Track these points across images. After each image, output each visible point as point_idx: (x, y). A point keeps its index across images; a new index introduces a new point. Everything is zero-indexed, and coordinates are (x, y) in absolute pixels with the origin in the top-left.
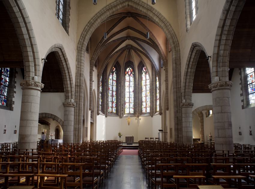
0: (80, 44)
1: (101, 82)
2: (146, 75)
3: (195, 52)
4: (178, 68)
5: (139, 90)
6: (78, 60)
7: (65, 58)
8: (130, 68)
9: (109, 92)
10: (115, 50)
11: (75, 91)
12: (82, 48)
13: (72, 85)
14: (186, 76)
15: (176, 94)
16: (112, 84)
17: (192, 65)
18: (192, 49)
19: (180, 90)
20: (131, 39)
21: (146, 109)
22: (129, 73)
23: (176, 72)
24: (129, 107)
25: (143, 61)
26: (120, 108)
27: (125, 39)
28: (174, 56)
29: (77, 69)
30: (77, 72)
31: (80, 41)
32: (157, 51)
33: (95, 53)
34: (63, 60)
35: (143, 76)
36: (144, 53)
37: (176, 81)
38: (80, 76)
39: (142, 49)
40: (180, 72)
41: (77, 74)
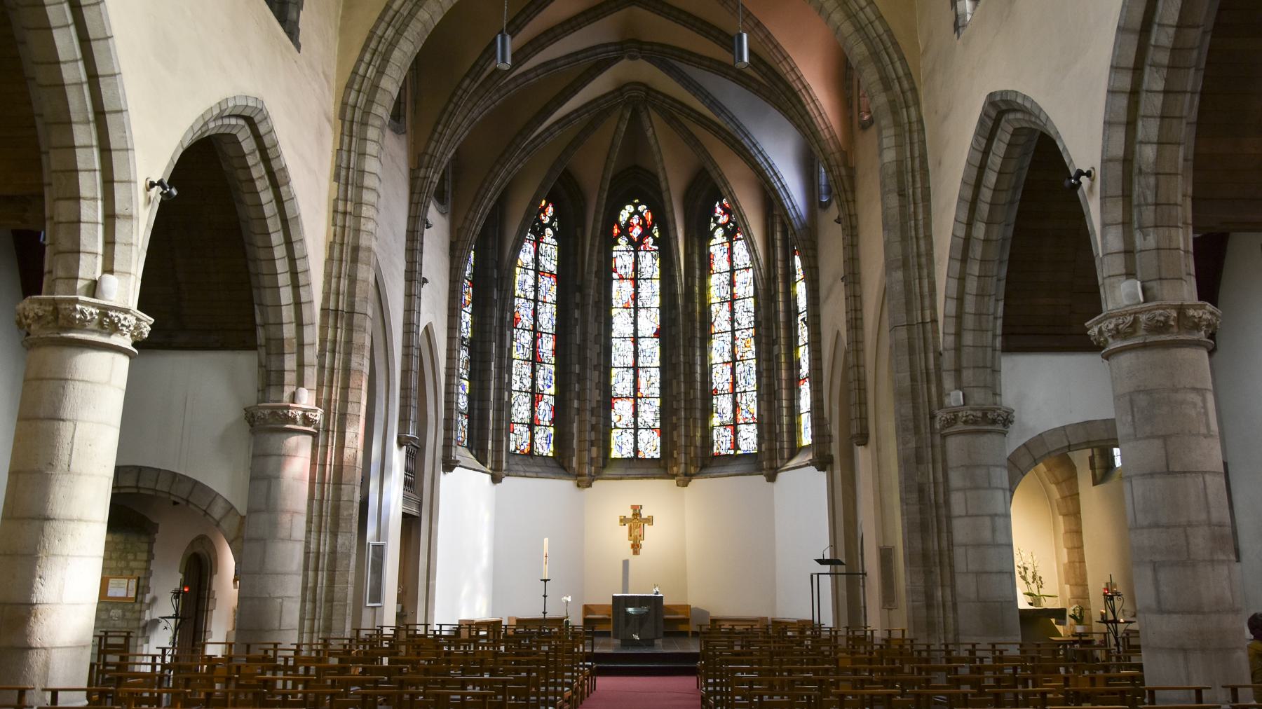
0: (356, 87)
3: (1004, 136)
4: (916, 220)
5: (694, 328)
6: (343, 173)
7: (275, 166)
8: (636, 206)
9: (512, 339)
11: (323, 341)
12: (367, 113)
13: (305, 309)
14: (964, 260)
15: (907, 357)
17: (993, 204)
18: (990, 124)
19: (930, 335)
20: (643, 58)
21: (735, 433)
22: (636, 232)
23: (904, 239)
24: (636, 423)
25: (716, 167)
26: (580, 431)
27: (613, 54)
28: (890, 156)
29: (335, 225)
30: (338, 240)
31: (361, 71)
32: (791, 119)
33: (440, 128)
34: (262, 177)
35: (712, 250)
36: (719, 126)
37: (907, 284)
38: (355, 260)
39: (709, 107)
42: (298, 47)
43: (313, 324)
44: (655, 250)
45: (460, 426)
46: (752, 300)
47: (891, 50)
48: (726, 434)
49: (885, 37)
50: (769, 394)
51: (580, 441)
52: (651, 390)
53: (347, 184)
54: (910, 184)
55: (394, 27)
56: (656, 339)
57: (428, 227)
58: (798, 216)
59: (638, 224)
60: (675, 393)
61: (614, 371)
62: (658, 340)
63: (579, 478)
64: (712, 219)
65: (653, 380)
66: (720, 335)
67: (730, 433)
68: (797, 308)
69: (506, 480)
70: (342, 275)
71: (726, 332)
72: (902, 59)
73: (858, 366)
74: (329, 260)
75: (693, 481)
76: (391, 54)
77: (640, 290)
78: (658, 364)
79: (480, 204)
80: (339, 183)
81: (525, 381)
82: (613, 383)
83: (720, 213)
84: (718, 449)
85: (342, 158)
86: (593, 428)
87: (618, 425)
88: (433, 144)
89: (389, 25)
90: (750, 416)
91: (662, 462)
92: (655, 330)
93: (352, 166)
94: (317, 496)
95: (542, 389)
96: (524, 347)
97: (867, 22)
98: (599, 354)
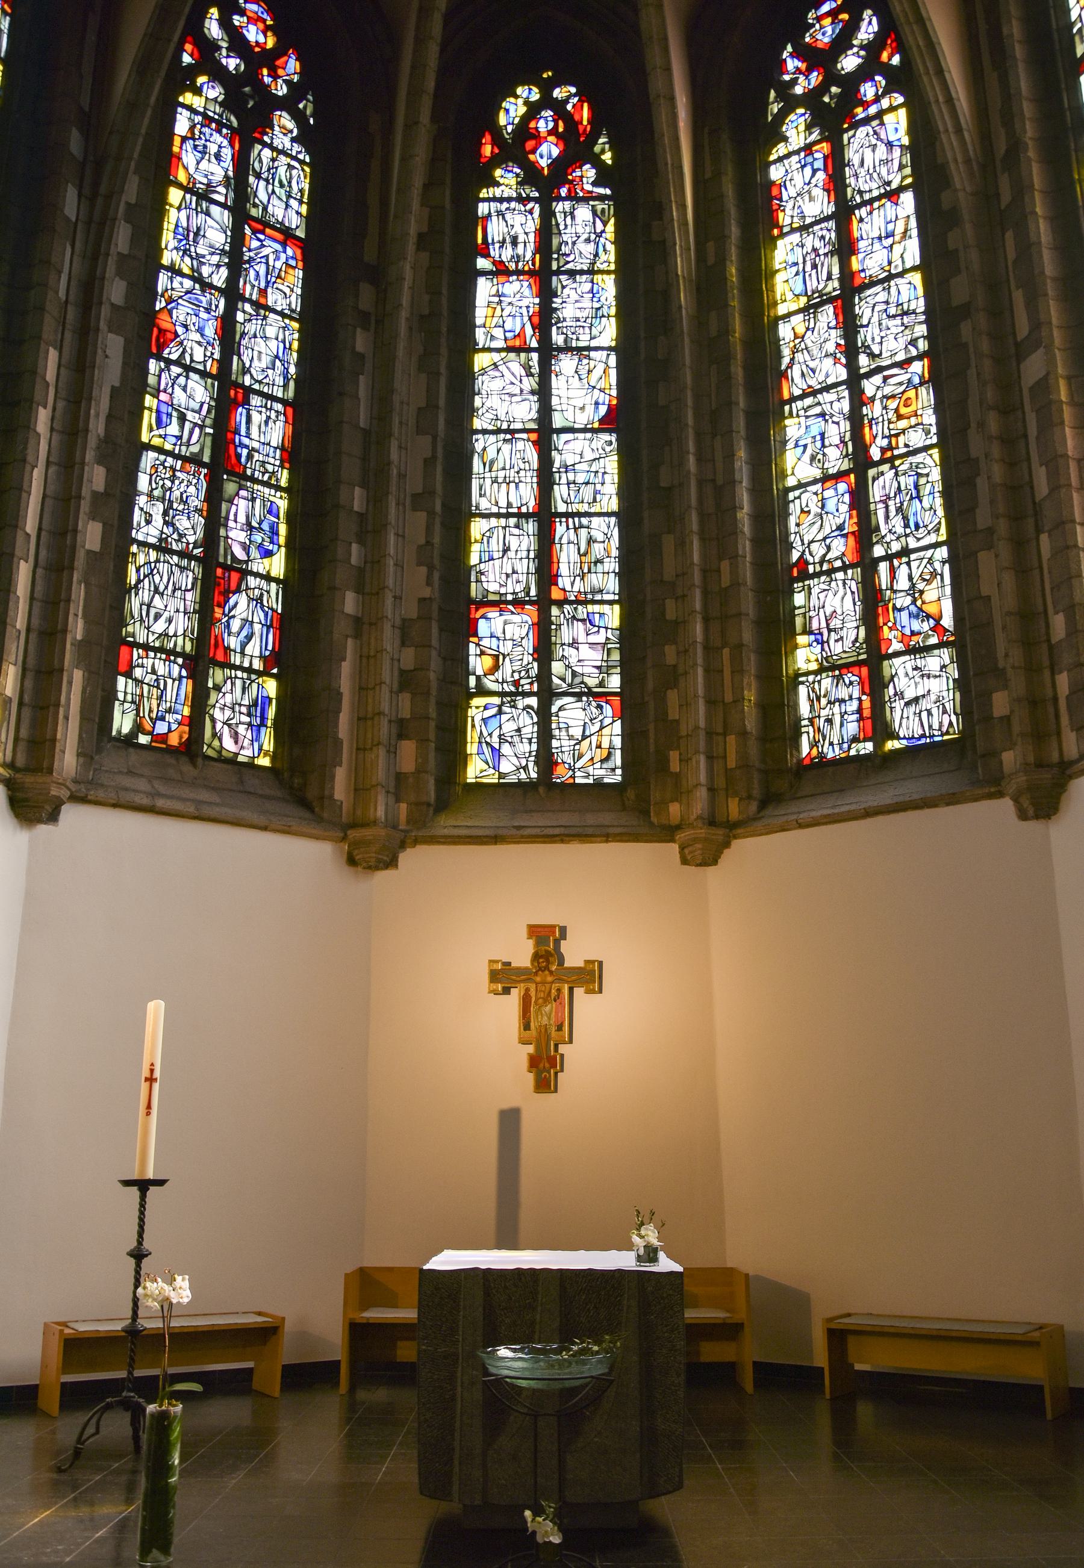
5: (726, 378)
8: (546, 88)
22: (547, 153)
24: (544, 676)
44: (601, 198)
46: (917, 278)
48: (843, 693)
50: (1016, 518)
52: (595, 580)
56: (606, 437)
59: (553, 132)
60: (669, 574)
61: (477, 528)
62: (613, 438)
63: (353, 834)
64: (773, 94)
65: (598, 550)
66: (809, 401)
67: (856, 692)
71: (827, 389)
75: (736, 844)
78: (613, 504)
81: (183, 523)
82: (474, 559)
83: (798, 70)
84: (814, 744)
86: (407, 681)
91: (631, 794)
92: (603, 410)
95: (240, 554)
96: (182, 419)
98: (429, 463)
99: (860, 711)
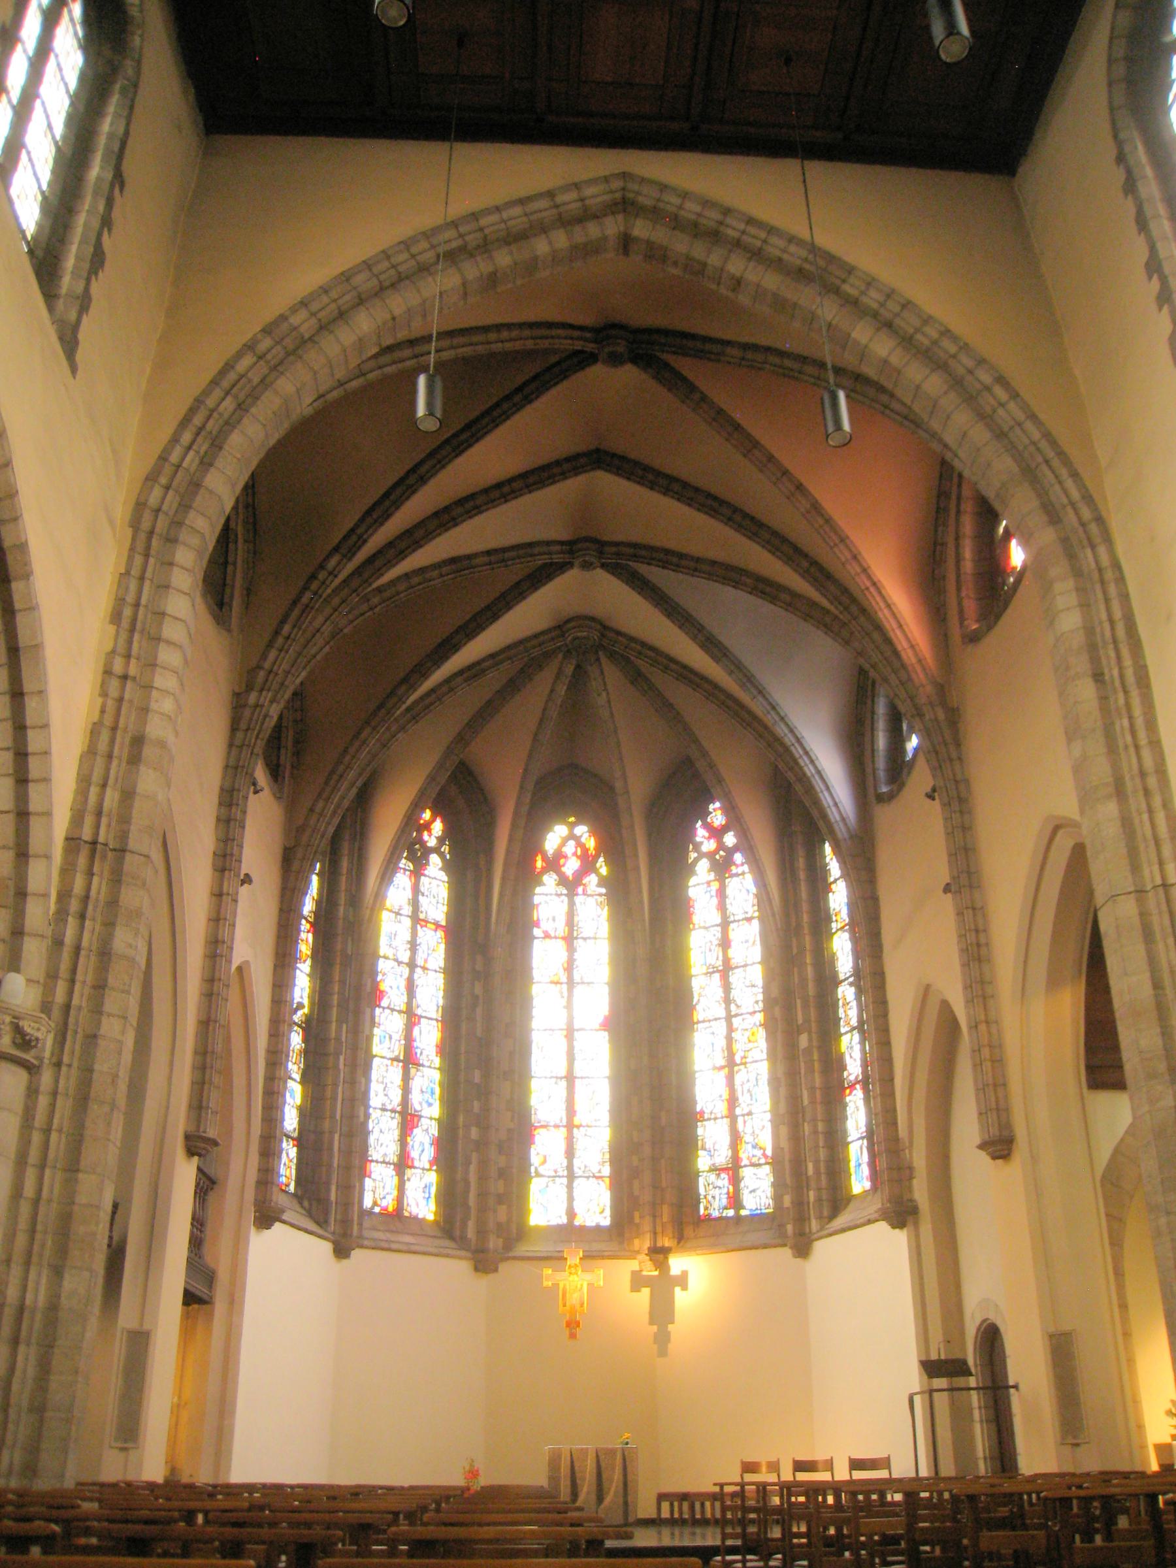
0: (163, 480)
1: (305, 926)
2: (721, 879)
4: (1131, 718)
6: (128, 612)
8: (572, 826)
9: (373, 1023)
10: (456, 648)
11: (64, 895)
12: (177, 523)
13: (35, 825)
16: (405, 956)
20: (603, 566)
21: (735, 1180)
22: (571, 866)
23: (1112, 748)
24: (570, 1167)
25: (705, 754)
26: (483, 1178)
27: (557, 558)
28: (1070, 621)
29: (104, 694)
30: (108, 720)
31: (174, 457)
33: (287, 628)
35: (692, 892)
37: (1127, 823)
38: (135, 759)
40: (1156, 744)
41: (105, 736)
42: (74, 369)
43: (48, 857)
44: (600, 895)
45: (284, 1158)
47: (1056, 463)
48: (720, 1183)
49: (1044, 445)
51: (483, 1195)
53: (132, 630)
54: (1113, 662)
55: (236, 397)
57: (256, 792)
58: (843, 819)
59: (575, 854)
66: (707, 1024)
67: (726, 1182)
68: (835, 974)
69: (356, 1254)
70: (111, 782)
72: (1075, 475)
73: (987, 1022)
74: (90, 752)
76: (226, 439)
77: (576, 956)
79: (335, 789)
80: (119, 626)
84: (706, 1208)
85: (127, 588)
87: (542, 1170)
88: (273, 654)
89: (227, 393)
90: (759, 1153)
93: (144, 601)
94: (29, 1191)
95: (418, 1107)
96: (391, 1037)
97: (1012, 423)
99: (728, 1193)
